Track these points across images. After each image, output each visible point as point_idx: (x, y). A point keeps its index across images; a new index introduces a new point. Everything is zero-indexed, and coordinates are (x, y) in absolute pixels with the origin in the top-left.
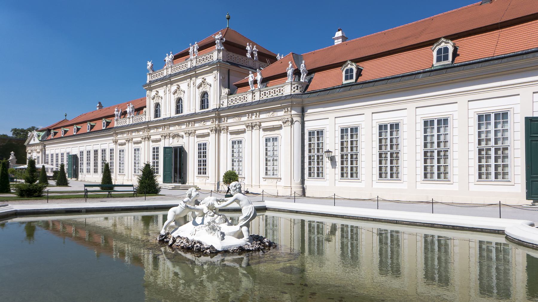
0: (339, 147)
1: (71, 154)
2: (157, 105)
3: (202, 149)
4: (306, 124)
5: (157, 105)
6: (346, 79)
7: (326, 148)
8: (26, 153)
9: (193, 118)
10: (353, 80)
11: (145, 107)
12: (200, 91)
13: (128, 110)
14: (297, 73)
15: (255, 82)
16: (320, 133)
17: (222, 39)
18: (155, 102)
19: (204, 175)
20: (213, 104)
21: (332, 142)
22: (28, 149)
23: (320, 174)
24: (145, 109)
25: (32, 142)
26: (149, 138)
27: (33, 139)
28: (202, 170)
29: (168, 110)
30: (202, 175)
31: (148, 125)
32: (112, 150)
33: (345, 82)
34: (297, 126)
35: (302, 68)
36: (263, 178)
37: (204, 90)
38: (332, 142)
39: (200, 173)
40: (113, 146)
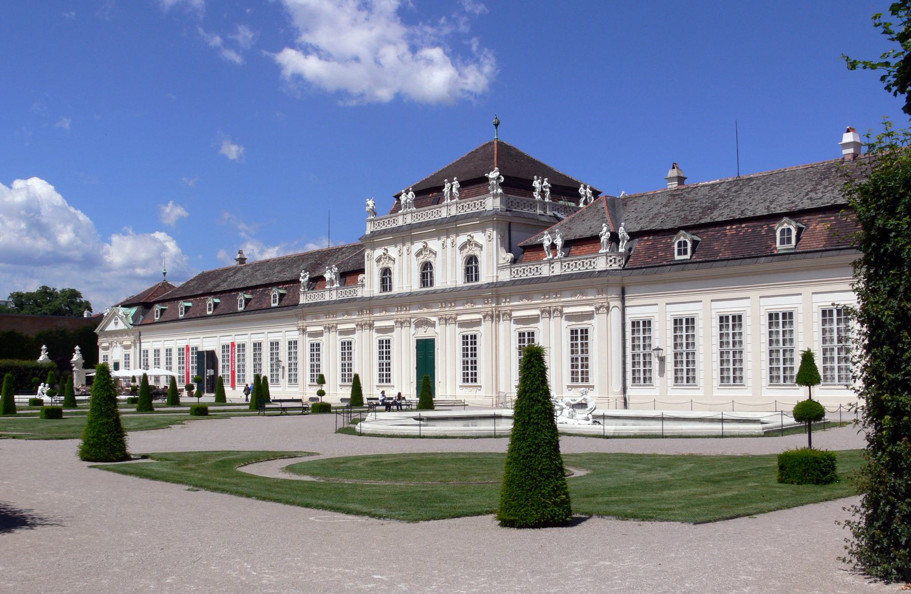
0: (670, 342)
1: (200, 349)
2: (386, 272)
3: (470, 345)
4: (628, 310)
5: (386, 272)
6: (680, 253)
7: (655, 343)
8: (97, 348)
9: (451, 296)
10: (688, 257)
11: (362, 271)
12: (465, 255)
13: (327, 276)
14: (614, 238)
15: (553, 246)
16: (647, 323)
17: (499, 178)
18: (381, 266)
19: (474, 384)
20: (487, 275)
21: (662, 337)
22: (102, 342)
23: (647, 380)
24: (360, 277)
25: (111, 327)
26: (371, 326)
27: (113, 321)
28: (470, 375)
29: (406, 280)
30: (470, 384)
31: (368, 305)
32: (293, 344)
33: (677, 257)
34: (616, 313)
35: (622, 232)
36: (568, 387)
37: (471, 253)
38: (662, 337)
39: (466, 380)
40: (294, 335)
